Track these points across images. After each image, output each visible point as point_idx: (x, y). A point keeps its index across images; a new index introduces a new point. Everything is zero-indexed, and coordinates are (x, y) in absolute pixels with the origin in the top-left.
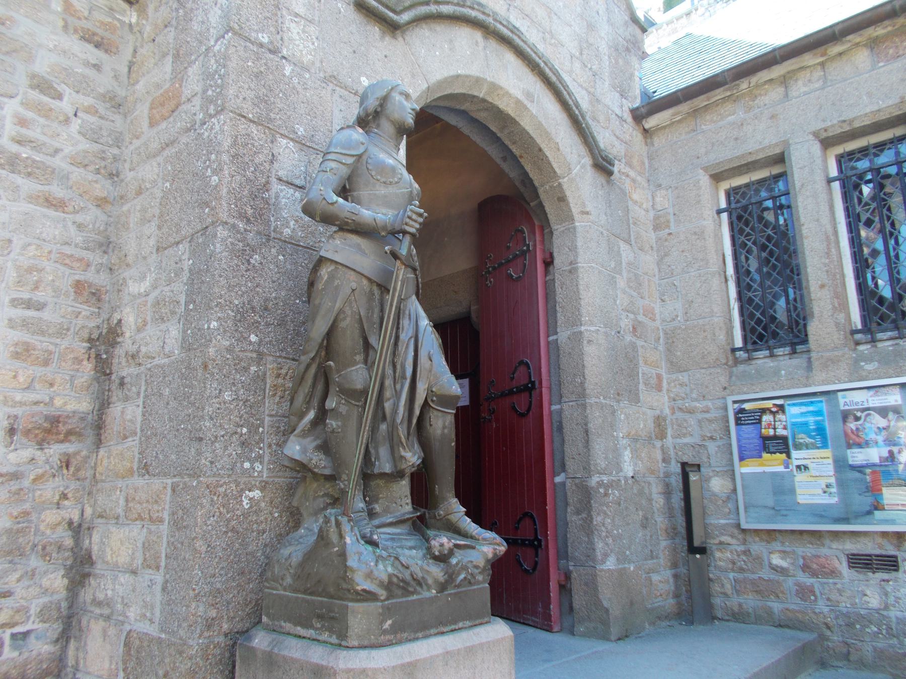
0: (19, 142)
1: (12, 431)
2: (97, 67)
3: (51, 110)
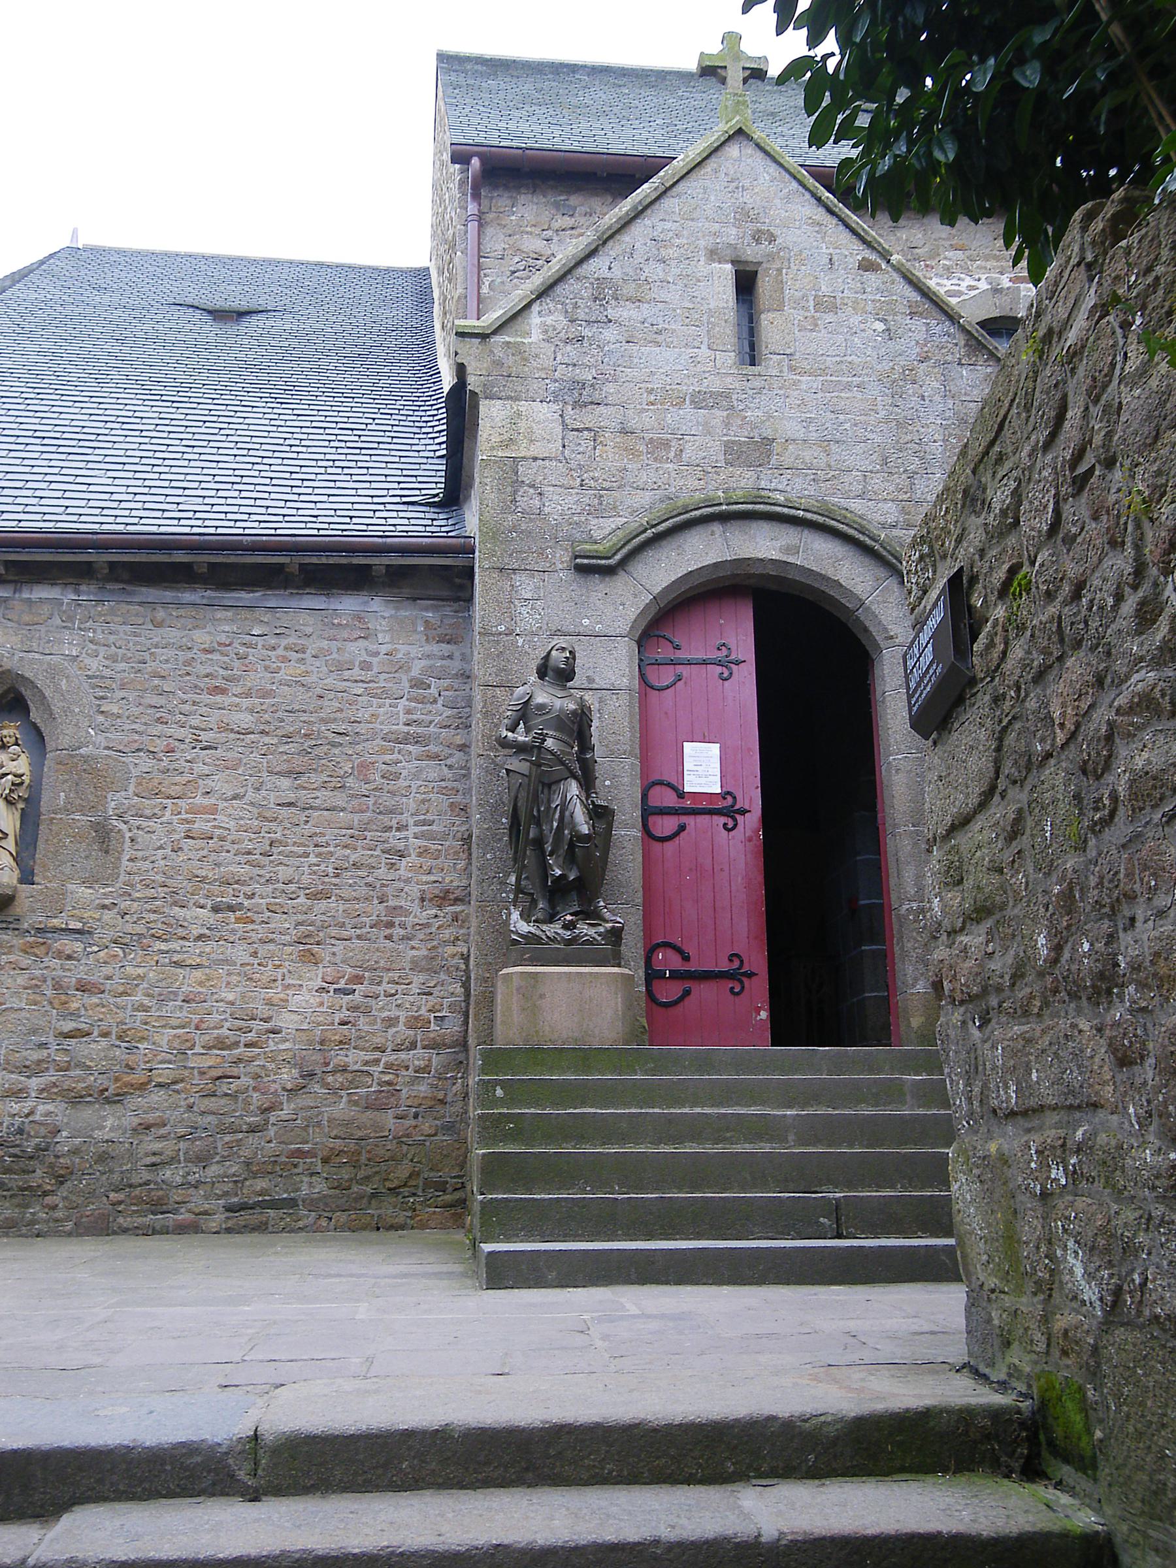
0: (408, 724)
1: (423, 900)
2: (450, 657)
3: (425, 697)
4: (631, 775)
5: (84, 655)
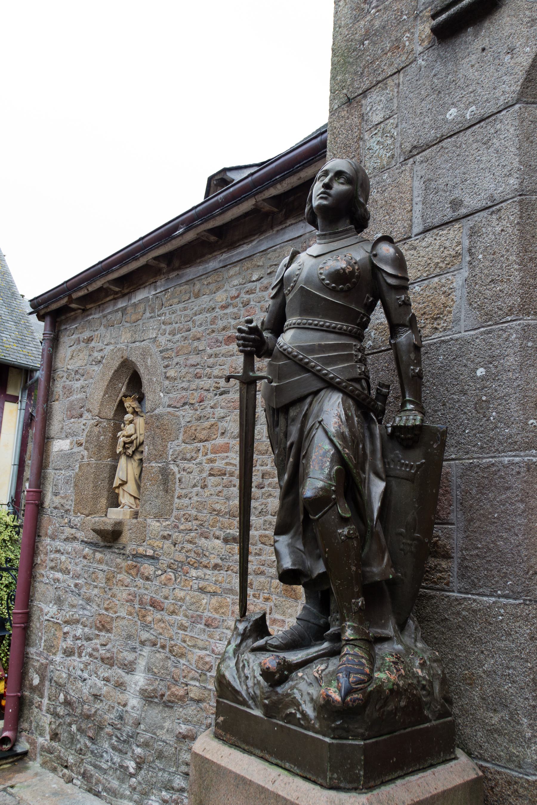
4: (523, 348)
5: (159, 336)
